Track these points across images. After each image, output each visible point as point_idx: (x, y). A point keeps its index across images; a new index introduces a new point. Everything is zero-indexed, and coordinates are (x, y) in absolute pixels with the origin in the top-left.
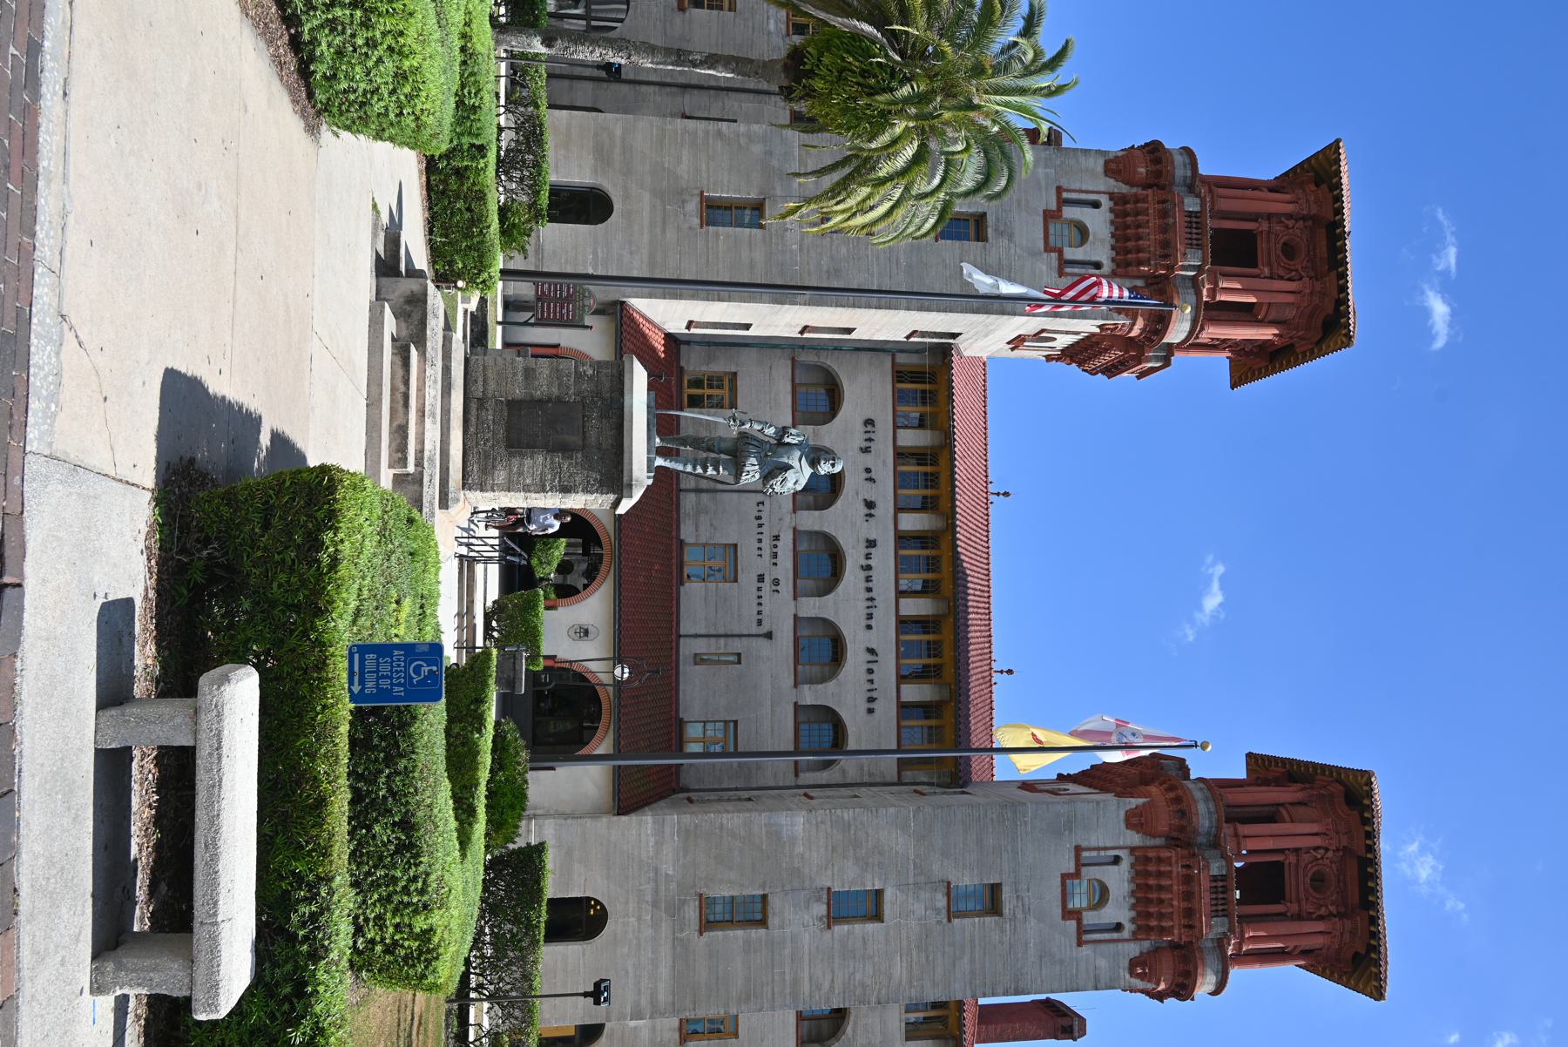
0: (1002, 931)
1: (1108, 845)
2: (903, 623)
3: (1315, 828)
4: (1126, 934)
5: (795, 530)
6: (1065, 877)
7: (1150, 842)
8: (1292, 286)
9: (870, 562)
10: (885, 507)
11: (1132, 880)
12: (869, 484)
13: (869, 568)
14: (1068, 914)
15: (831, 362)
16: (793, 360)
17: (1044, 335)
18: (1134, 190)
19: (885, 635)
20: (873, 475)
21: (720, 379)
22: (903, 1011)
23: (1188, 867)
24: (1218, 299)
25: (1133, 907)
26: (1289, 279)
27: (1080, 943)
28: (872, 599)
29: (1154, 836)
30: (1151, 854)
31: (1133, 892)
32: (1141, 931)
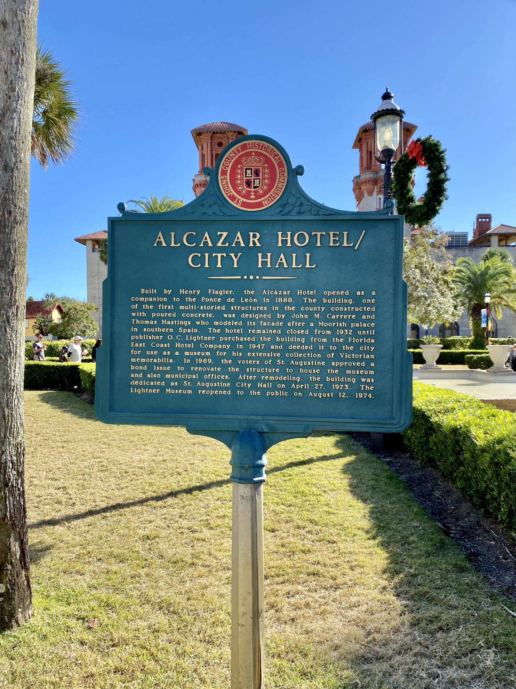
7: (376, 190)
30: (379, 190)
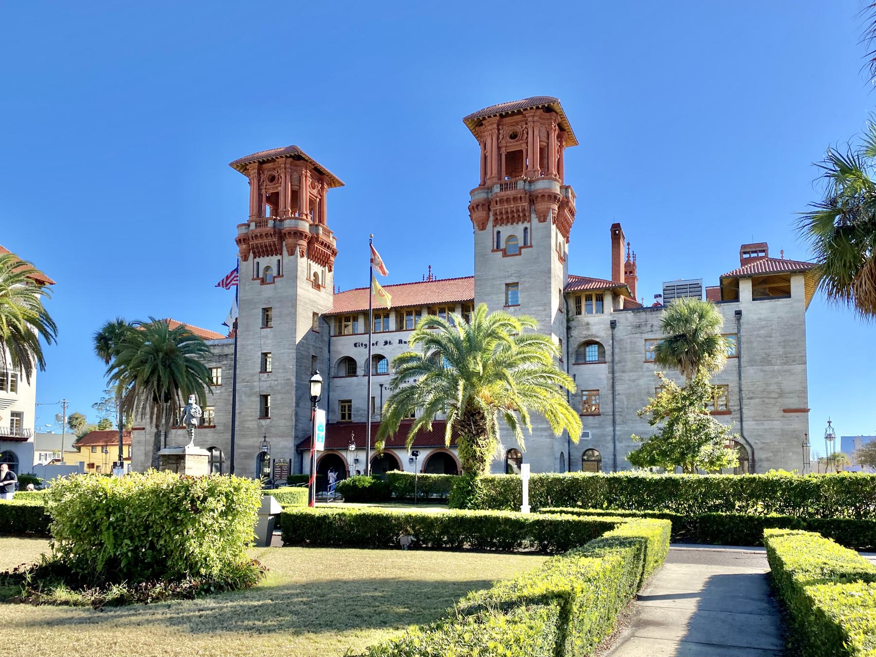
0: (524, 282)
6: (505, 255)
12: (378, 344)
15: (334, 361)
16: (334, 377)
17: (312, 278)
20: (375, 342)
21: (342, 407)
22: (591, 315)
23: (496, 202)
25: (518, 223)
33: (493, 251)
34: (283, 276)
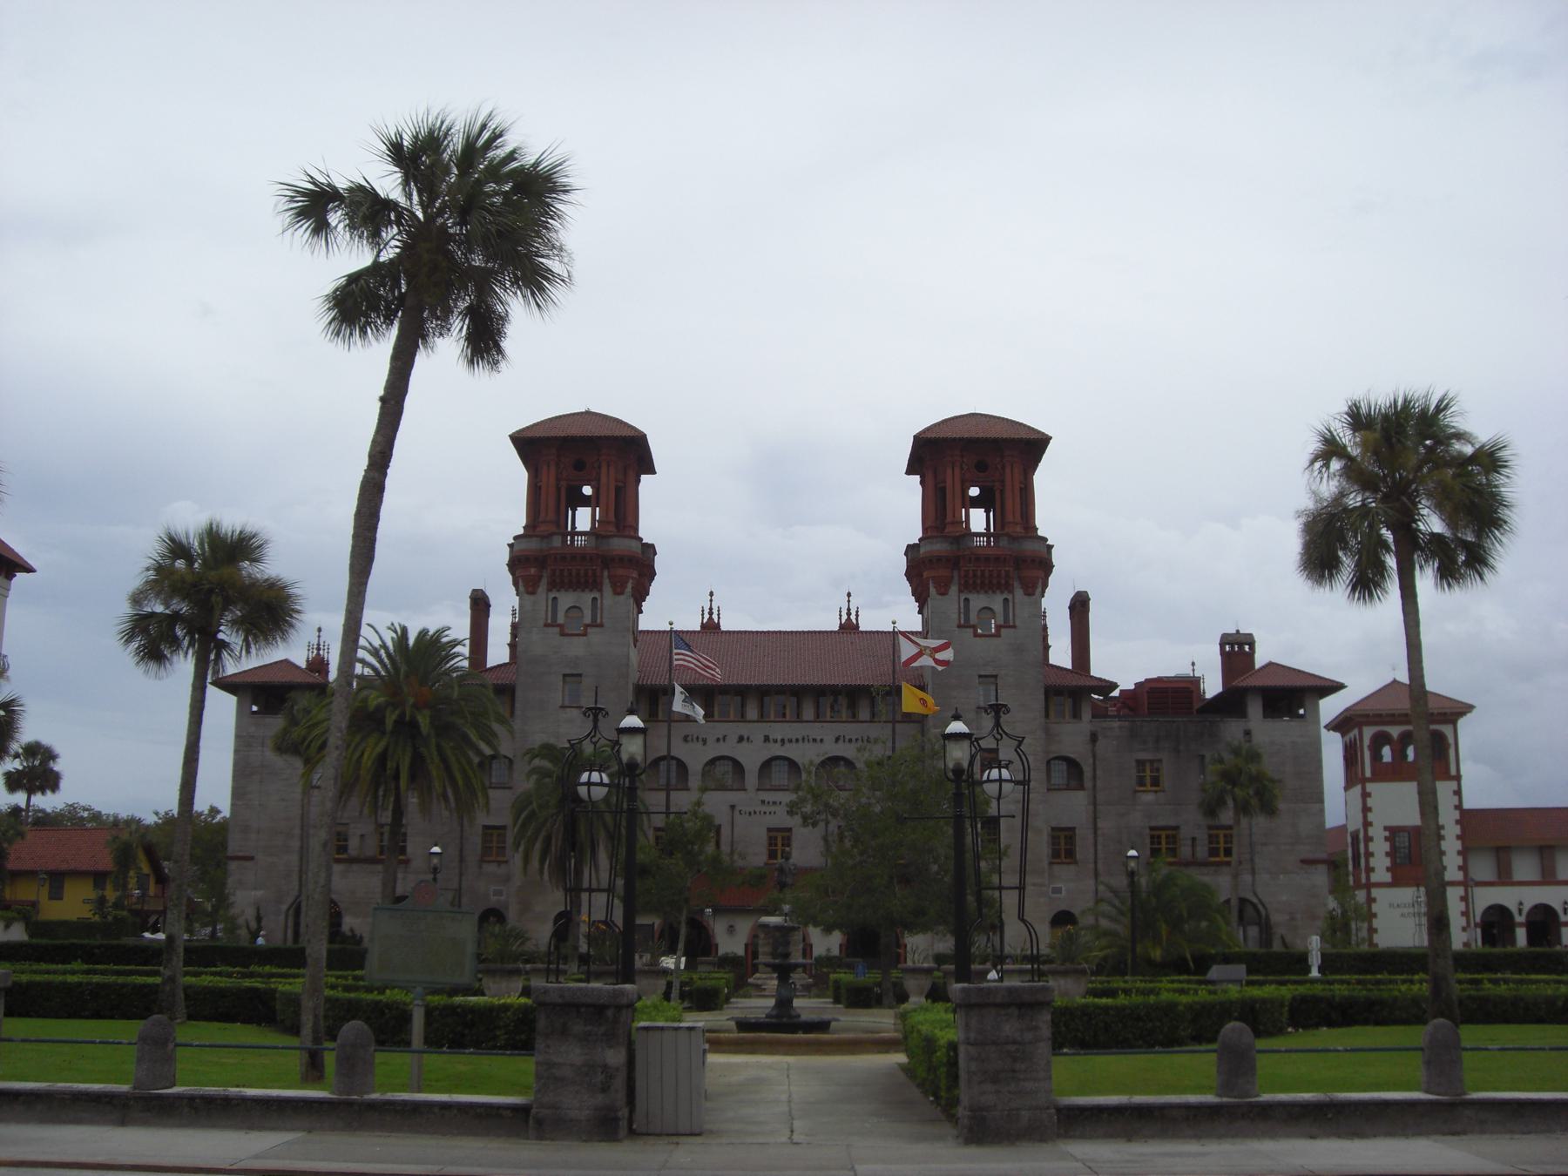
1: (957, 607)
2: (818, 718)
3: (949, 471)
4: (1010, 597)
5: (758, 790)
8: (604, 470)
9: (779, 740)
10: (743, 729)
11: (978, 592)
12: (727, 738)
13: (783, 740)
14: (997, 635)
18: (545, 574)
19: (827, 731)
20: (721, 737)
24: (613, 519)
25: (994, 592)
26: (600, 467)
27: (1014, 627)
28: (803, 739)
29: (952, 577)
31: (986, 592)
32: (1008, 587)
33: (959, 626)
34: (601, 625)
